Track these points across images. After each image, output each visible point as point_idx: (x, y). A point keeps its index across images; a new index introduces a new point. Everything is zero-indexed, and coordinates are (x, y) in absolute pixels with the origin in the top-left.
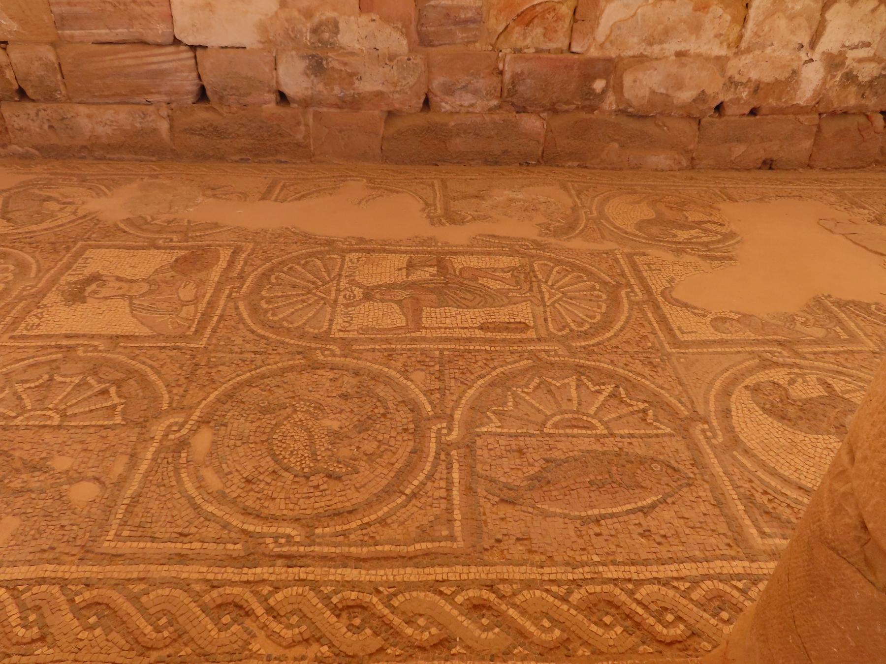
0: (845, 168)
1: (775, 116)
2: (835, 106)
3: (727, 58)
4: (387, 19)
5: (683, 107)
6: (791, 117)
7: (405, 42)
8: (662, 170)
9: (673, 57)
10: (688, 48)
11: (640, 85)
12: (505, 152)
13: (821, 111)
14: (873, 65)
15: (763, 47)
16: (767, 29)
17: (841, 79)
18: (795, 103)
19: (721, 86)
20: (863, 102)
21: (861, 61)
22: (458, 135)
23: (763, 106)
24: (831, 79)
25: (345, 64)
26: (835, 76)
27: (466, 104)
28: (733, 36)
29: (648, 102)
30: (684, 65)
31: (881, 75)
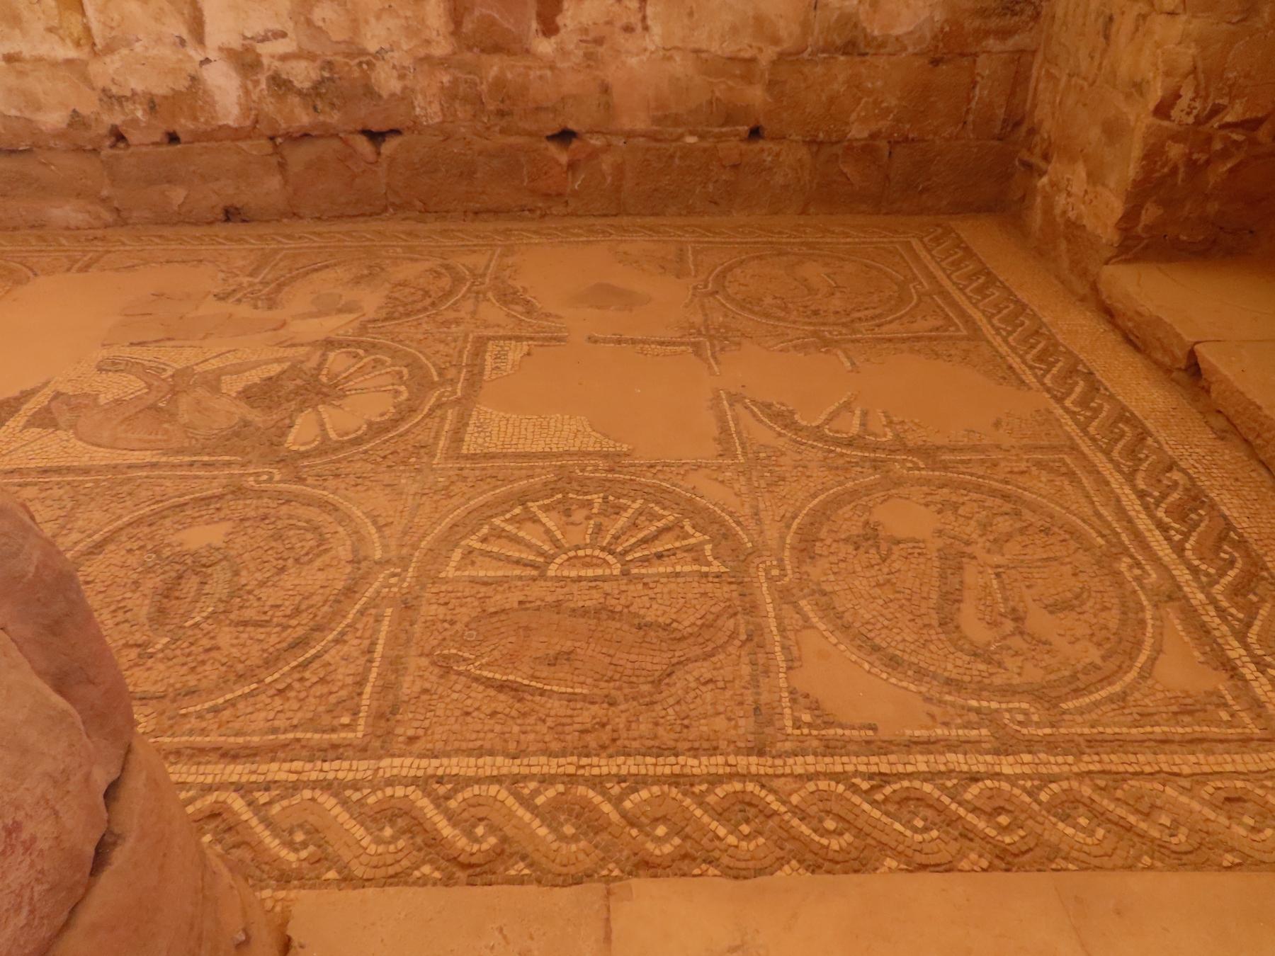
0: (349, 216)
1: (205, 144)
2: (284, 126)
5: (60, 135)
6: (228, 143)
8: (78, 229)
10: (17, 49)
13: (269, 133)
14: (303, 64)
15: (129, 44)
16: (116, 16)
17: (269, 87)
18: (221, 123)
19: (97, 102)
20: (321, 118)
21: (284, 58)
23: (177, 127)
24: (255, 87)
26: (256, 83)
28: (77, 30)
30: (21, 74)
31: (322, 81)
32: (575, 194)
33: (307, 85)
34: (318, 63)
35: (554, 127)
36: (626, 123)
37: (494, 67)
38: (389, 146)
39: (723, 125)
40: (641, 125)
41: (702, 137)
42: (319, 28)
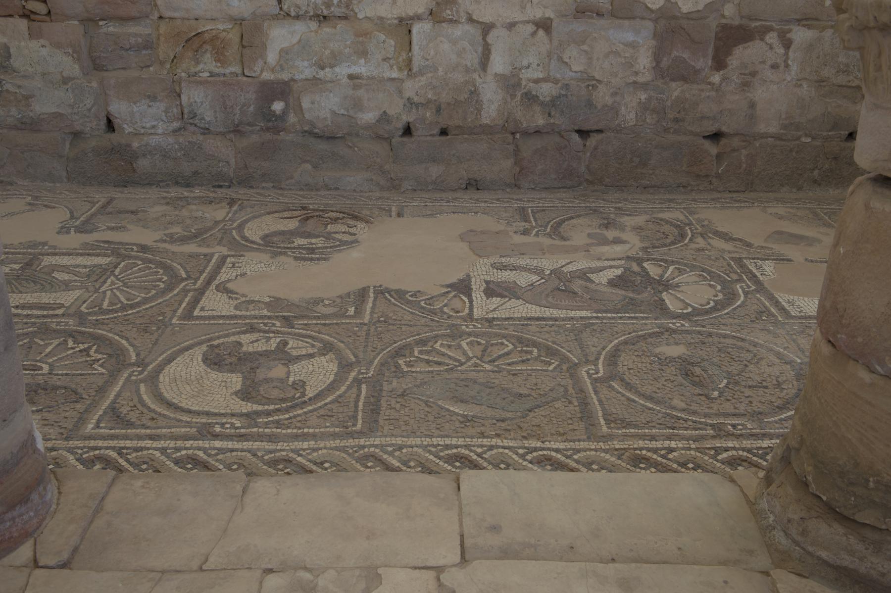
2: (524, 125)
3: (402, 81)
4: (58, 45)
7: (77, 66)
9: (345, 80)
11: (322, 107)
12: (196, 173)
14: (551, 85)
16: (432, 52)
20: (552, 121)
21: (537, 81)
22: (144, 155)
25: (19, 87)
27: (148, 125)
29: (332, 122)
31: (559, 96)
32: (718, 176)
33: (548, 99)
34: (560, 85)
35: (712, 128)
36: (762, 128)
37: (676, 90)
38: (593, 141)
39: (830, 131)
40: (772, 130)
41: (813, 138)
42: (566, 63)
